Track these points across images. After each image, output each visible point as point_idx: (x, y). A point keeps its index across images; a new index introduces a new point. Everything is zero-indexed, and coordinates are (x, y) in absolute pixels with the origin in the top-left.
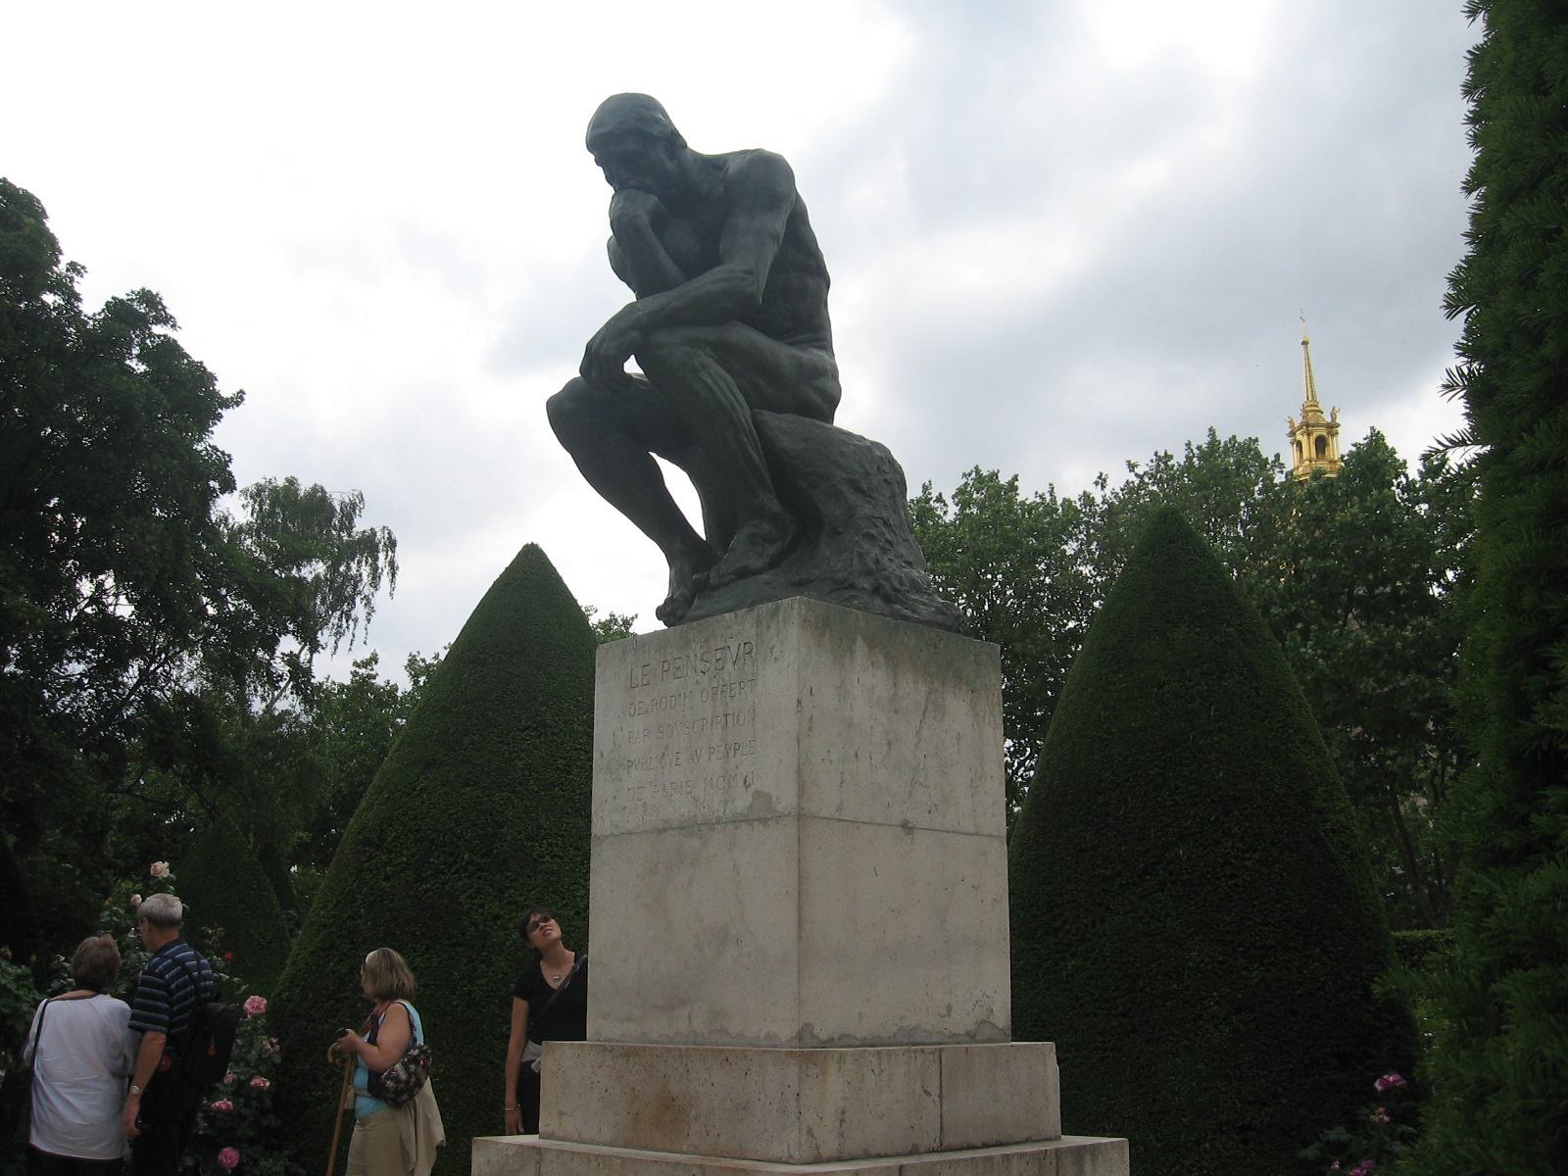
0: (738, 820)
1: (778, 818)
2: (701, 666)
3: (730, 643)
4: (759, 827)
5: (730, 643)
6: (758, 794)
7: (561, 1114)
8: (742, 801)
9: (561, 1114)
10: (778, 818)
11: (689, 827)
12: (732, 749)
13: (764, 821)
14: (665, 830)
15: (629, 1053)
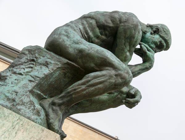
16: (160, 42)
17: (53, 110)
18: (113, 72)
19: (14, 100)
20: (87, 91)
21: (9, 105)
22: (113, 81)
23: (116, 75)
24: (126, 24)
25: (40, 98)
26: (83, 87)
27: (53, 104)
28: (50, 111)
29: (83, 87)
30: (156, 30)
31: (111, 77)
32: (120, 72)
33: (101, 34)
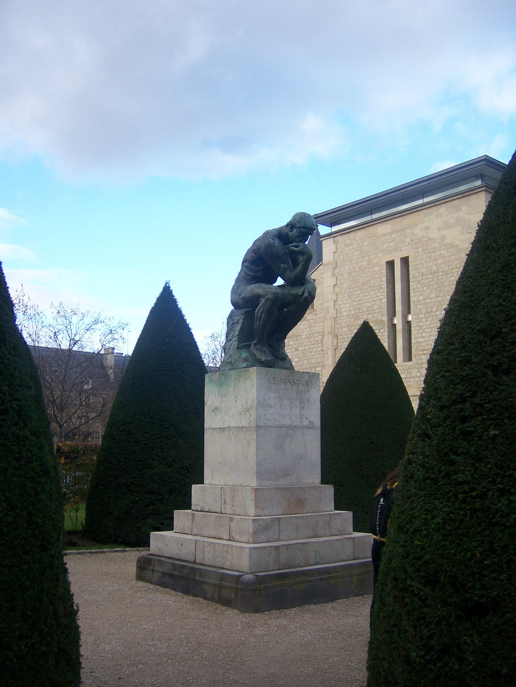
0: (304, 427)
1: (315, 428)
2: (292, 383)
3: (301, 379)
4: (310, 430)
5: (301, 379)
6: (309, 421)
7: (263, 509)
8: (306, 423)
9: (263, 509)
10: (315, 428)
11: (290, 427)
12: (302, 408)
13: (312, 428)
14: (282, 427)
15: (286, 489)
16: (300, 232)
17: (256, 349)
18: (263, 301)
19: (231, 362)
20: (261, 324)
21: (230, 367)
22: (266, 307)
23: (266, 301)
24: (262, 249)
25: (248, 347)
26: (258, 323)
27: (255, 345)
28: (255, 352)
29: (258, 323)
30: (291, 225)
31: (264, 304)
32: (266, 297)
33: (258, 267)
